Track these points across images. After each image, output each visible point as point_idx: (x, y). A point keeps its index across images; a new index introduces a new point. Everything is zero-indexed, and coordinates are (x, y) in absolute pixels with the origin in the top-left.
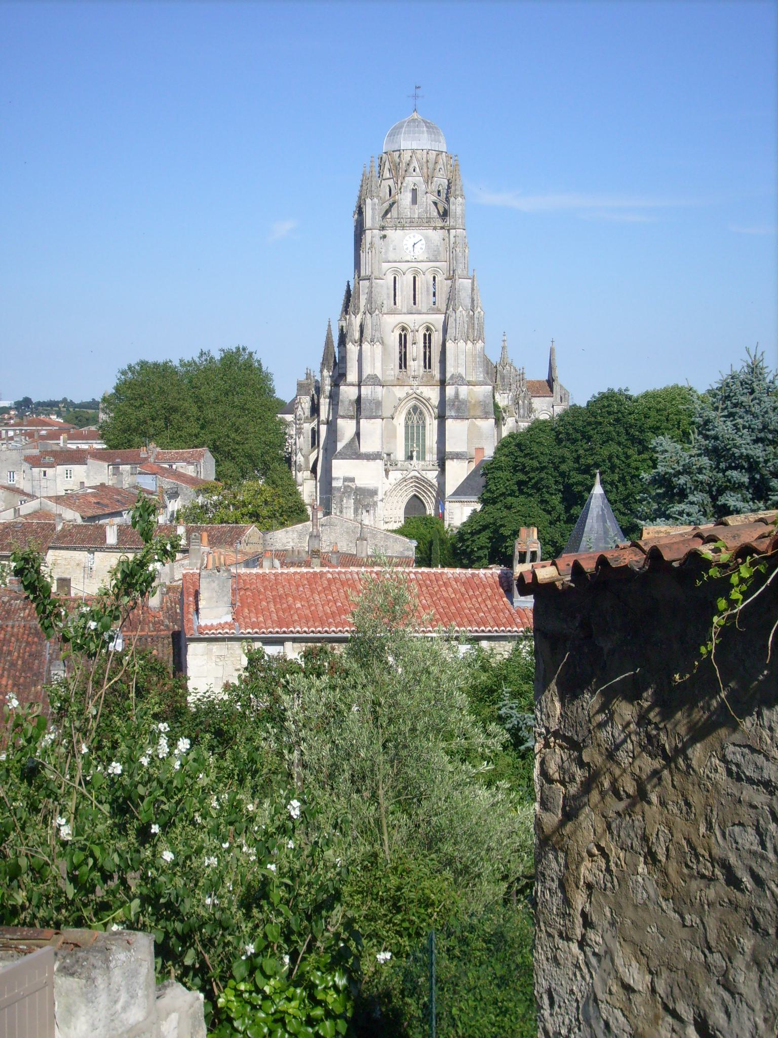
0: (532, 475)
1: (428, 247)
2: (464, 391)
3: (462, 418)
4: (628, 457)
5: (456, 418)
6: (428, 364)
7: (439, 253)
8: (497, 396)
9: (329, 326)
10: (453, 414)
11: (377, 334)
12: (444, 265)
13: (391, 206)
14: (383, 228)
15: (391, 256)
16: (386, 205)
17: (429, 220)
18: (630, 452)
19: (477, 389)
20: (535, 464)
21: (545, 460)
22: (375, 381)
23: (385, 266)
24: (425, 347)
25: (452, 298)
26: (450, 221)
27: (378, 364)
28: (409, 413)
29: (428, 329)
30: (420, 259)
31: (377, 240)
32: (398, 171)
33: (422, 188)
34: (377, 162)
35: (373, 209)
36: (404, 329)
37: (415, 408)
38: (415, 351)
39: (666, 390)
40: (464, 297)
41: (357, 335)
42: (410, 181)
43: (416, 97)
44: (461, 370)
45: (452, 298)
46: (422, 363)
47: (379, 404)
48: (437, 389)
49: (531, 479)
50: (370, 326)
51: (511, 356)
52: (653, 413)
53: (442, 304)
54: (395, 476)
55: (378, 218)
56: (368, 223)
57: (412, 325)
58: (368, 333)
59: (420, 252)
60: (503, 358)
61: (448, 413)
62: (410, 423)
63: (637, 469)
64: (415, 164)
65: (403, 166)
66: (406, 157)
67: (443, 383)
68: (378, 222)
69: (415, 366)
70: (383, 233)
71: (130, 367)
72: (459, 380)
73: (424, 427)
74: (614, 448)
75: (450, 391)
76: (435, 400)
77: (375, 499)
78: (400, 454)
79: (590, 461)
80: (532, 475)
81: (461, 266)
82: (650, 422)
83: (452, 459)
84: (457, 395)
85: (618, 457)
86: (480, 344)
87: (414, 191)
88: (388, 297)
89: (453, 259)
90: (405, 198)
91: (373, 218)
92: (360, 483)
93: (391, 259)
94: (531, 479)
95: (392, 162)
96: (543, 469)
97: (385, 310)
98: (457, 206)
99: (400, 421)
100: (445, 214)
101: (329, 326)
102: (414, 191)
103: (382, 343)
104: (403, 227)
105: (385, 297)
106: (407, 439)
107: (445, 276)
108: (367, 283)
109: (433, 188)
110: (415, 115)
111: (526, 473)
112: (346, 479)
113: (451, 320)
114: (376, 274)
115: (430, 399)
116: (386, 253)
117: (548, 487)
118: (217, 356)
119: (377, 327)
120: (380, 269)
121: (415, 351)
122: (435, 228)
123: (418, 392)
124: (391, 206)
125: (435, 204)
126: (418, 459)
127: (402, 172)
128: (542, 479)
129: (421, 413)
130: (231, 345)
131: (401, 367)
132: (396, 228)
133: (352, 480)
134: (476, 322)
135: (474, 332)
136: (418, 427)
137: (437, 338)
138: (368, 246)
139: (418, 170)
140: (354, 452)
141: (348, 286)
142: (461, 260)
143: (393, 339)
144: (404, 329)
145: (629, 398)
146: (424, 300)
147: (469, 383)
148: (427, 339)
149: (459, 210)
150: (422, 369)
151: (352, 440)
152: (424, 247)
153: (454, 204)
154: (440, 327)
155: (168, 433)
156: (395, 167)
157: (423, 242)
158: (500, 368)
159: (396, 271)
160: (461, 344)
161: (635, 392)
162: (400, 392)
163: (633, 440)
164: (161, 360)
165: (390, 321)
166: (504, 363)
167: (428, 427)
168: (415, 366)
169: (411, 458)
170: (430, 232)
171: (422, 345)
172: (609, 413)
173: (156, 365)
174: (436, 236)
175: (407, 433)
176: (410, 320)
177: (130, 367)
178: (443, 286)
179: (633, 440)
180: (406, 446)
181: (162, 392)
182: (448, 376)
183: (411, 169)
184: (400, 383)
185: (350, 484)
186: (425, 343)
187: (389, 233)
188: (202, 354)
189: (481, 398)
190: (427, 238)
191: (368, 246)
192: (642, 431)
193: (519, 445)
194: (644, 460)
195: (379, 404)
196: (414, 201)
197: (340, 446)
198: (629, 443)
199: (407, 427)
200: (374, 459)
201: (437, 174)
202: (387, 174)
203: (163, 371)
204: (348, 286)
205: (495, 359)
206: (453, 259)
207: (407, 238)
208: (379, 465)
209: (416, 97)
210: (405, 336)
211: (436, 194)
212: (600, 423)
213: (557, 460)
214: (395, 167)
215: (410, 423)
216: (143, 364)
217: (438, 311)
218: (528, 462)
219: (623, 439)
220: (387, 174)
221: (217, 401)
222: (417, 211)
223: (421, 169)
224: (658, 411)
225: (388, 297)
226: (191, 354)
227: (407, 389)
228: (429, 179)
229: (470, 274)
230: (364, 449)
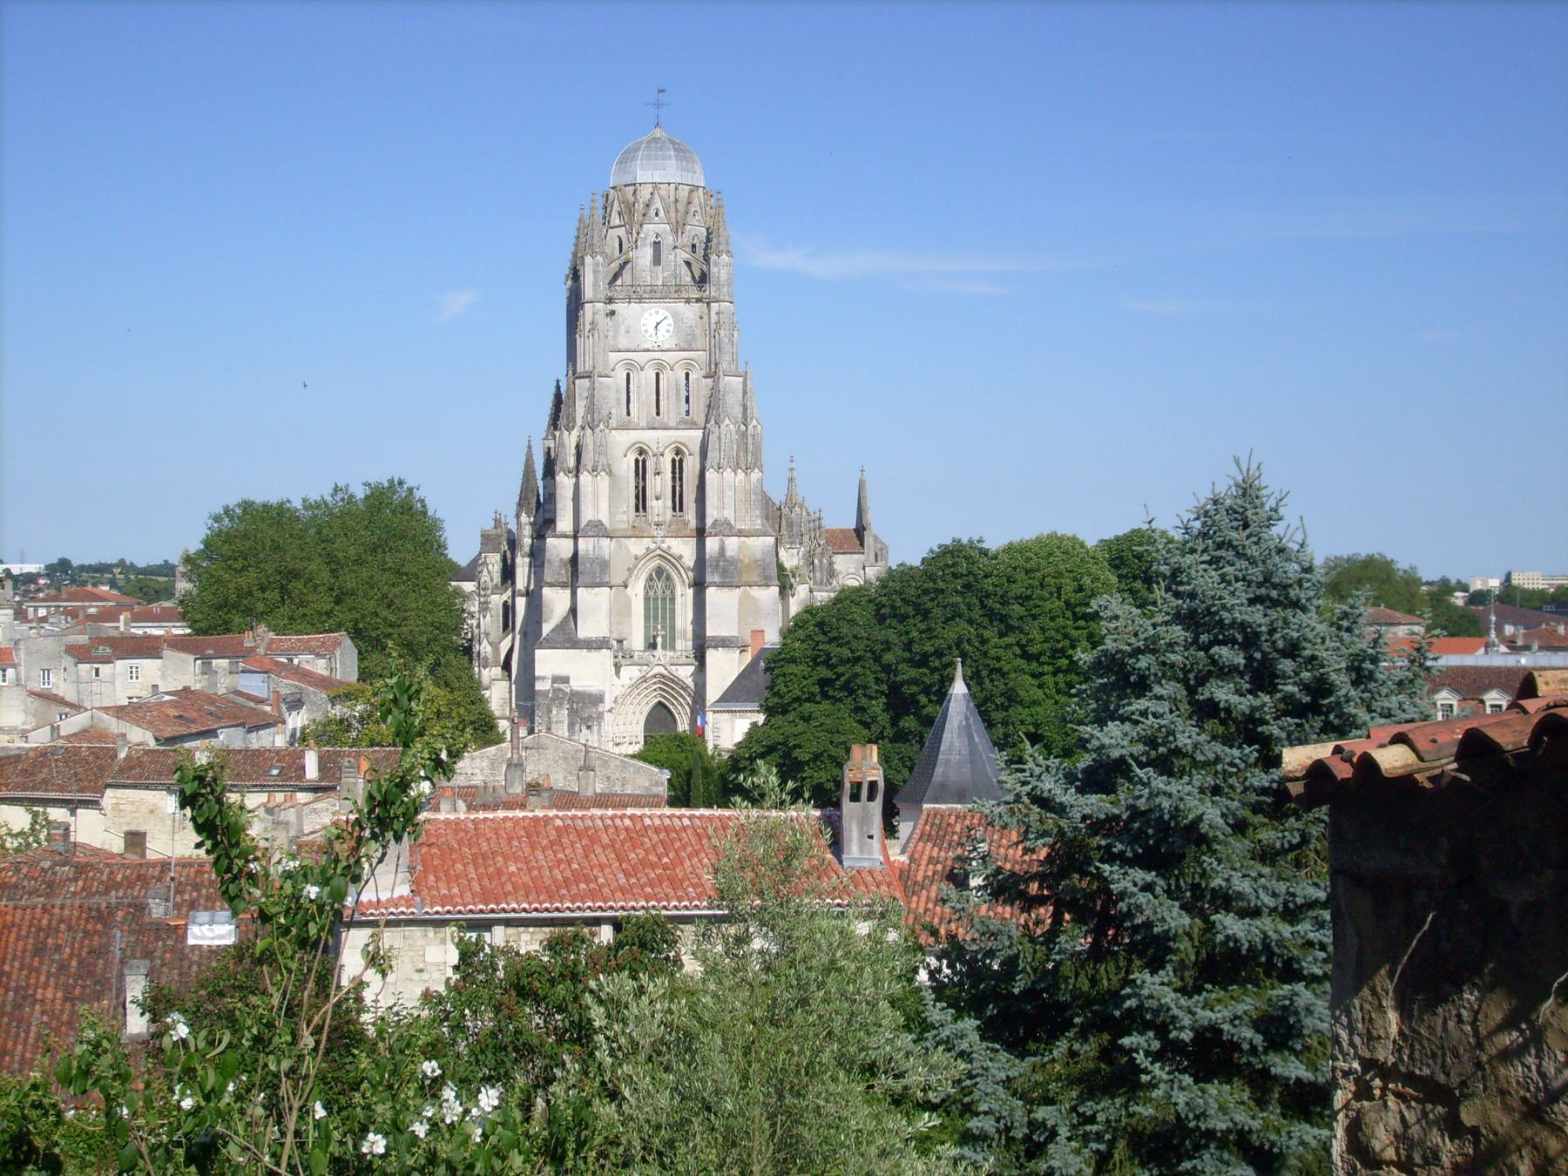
0: (840, 669)
1: (677, 329)
2: (732, 543)
3: (730, 586)
4: (984, 641)
5: (721, 585)
6: (678, 504)
7: (694, 336)
8: (782, 552)
9: (530, 447)
10: (717, 579)
11: (603, 460)
12: (701, 356)
13: (622, 267)
14: (610, 300)
15: (623, 342)
16: (615, 266)
17: (679, 288)
18: (987, 634)
19: (751, 541)
20: (846, 653)
21: (860, 647)
22: (598, 530)
23: (614, 357)
24: (674, 478)
25: (713, 405)
26: (711, 290)
27: (604, 505)
28: (650, 578)
29: (678, 452)
30: (666, 346)
31: (601, 318)
32: (634, 215)
33: (669, 240)
34: (602, 201)
35: (595, 272)
36: (641, 452)
37: (659, 571)
38: (660, 484)
39: (1038, 540)
40: (732, 404)
41: (572, 462)
42: (650, 230)
43: (658, 105)
44: (729, 514)
45: (713, 405)
46: (670, 504)
47: (605, 565)
48: (693, 542)
49: (839, 676)
50: (591, 448)
51: (801, 492)
52: (1020, 575)
53: (698, 414)
54: (630, 673)
55: (603, 285)
56: (588, 292)
57: (654, 447)
58: (588, 458)
59: (666, 336)
60: (790, 496)
61: (709, 579)
62: (651, 593)
63: (998, 659)
64: (658, 204)
65: (640, 207)
66: (645, 193)
67: (701, 533)
68: (604, 290)
69: (660, 507)
70: (610, 307)
71: (227, 511)
72: (726, 529)
73: (673, 599)
74: (962, 628)
75: (712, 544)
76: (689, 559)
78: (637, 641)
79: (929, 648)
80: (840, 669)
81: (727, 357)
82: (1017, 589)
83: (716, 647)
84: (722, 549)
85: (969, 641)
86: (755, 475)
87: (657, 245)
88: (619, 404)
89: (714, 349)
90: (644, 256)
91: (595, 284)
92: (576, 685)
93: (621, 346)
94: (839, 676)
95: (624, 202)
96: (859, 659)
97: (613, 423)
98: (721, 268)
99: (637, 590)
100: (703, 280)
101: (530, 447)
102: (657, 245)
103: (610, 473)
104: (640, 300)
105: (613, 403)
106: (647, 618)
107: (703, 373)
108: (586, 382)
109: (685, 240)
110: (658, 133)
111: (831, 667)
112: (556, 679)
113: (713, 438)
114: (600, 369)
115: (681, 557)
116: (615, 338)
117: (865, 687)
118: (360, 493)
119: (602, 449)
120: (606, 363)
121: (660, 484)
122: (688, 301)
123: (664, 546)
124: (622, 267)
125: (688, 264)
126: (664, 647)
127: (637, 217)
128: (856, 675)
129: (669, 578)
130: (382, 477)
131: (637, 510)
132: (629, 300)
133: (566, 680)
134: (750, 440)
135: (747, 456)
136: (664, 599)
137: (691, 465)
138: (588, 327)
139: (662, 213)
140: (567, 637)
141: (558, 387)
142: (727, 348)
143: (626, 467)
144: (641, 452)
145: (985, 553)
146: (672, 409)
147: (740, 534)
148: (677, 467)
149: (723, 276)
150: (669, 512)
151: (565, 620)
153: (716, 264)
154: (696, 449)
155: (285, 610)
156: (628, 210)
157: (671, 321)
158: (785, 511)
159: (630, 365)
160: (728, 474)
161: (993, 544)
162: (637, 547)
163: (992, 615)
164: (274, 499)
165: (622, 440)
166: (791, 502)
168: (660, 507)
169: (653, 646)
170: (681, 307)
171: (669, 475)
172: (955, 576)
173: (267, 507)
174: (690, 312)
175: (647, 609)
176: (651, 438)
177: (227, 511)
178: (700, 386)
179: (992, 615)
180: (647, 628)
181: (277, 548)
182: (709, 521)
183: (652, 212)
184: (636, 533)
185: (562, 686)
186: (674, 472)
187: (619, 307)
188: (336, 490)
189: (759, 556)
190: (675, 315)
191: (588, 327)
192: (1005, 603)
193: (820, 625)
194: (1008, 646)
195: (605, 565)
196: (657, 260)
197: (547, 628)
198: (986, 621)
199: (647, 599)
200: (599, 648)
201: (690, 219)
202: (616, 220)
203: (278, 515)
204: (558, 387)
205: (778, 496)
206: (714, 349)
207: (646, 315)
208: (606, 656)
209: (658, 105)
210: (644, 462)
211: (689, 249)
212: (942, 591)
213: (878, 647)
214: (628, 210)
215: (651, 593)
216: (247, 506)
217: (693, 425)
218: (834, 649)
219: (977, 614)
220: (616, 220)
221: (359, 562)
222: (661, 276)
223: (667, 212)
224: (1027, 572)
225: (619, 404)
226: (319, 491)
227: (646, 542)
228: (678, 227)
229: (741, 369)
230: (585, 631)
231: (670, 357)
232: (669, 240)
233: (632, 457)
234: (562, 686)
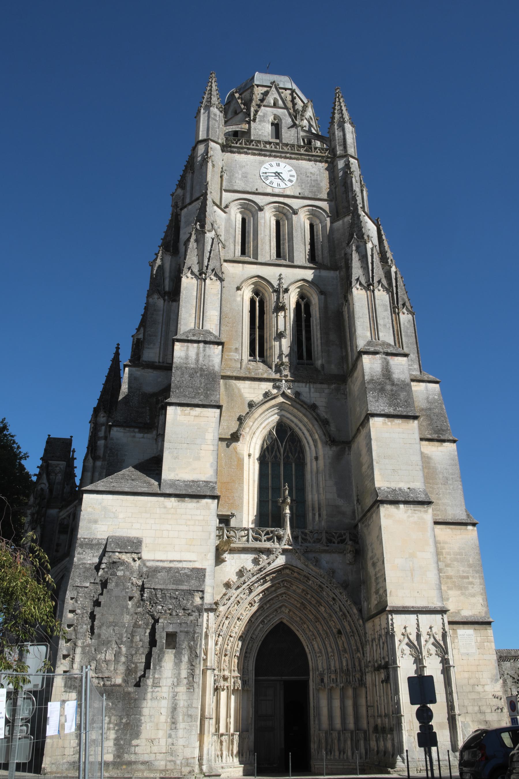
15: (239, 185)
23: (227, 197)
30: (288, 193)
73: (301, 464)
77: (197, 601)
93: (236, 188)
101: (117, 354)
115: (313, 407)
116: (230, 181)
133: (134, 546)
152: (294, 179)
167: (311, 466)
170: (305, 164)
185: (126, 558)
190: (298, 170)
210: (262, 303)
231: (295, 203)
232: (287, 121)
233: (247, 293)
234: (126, 558)
